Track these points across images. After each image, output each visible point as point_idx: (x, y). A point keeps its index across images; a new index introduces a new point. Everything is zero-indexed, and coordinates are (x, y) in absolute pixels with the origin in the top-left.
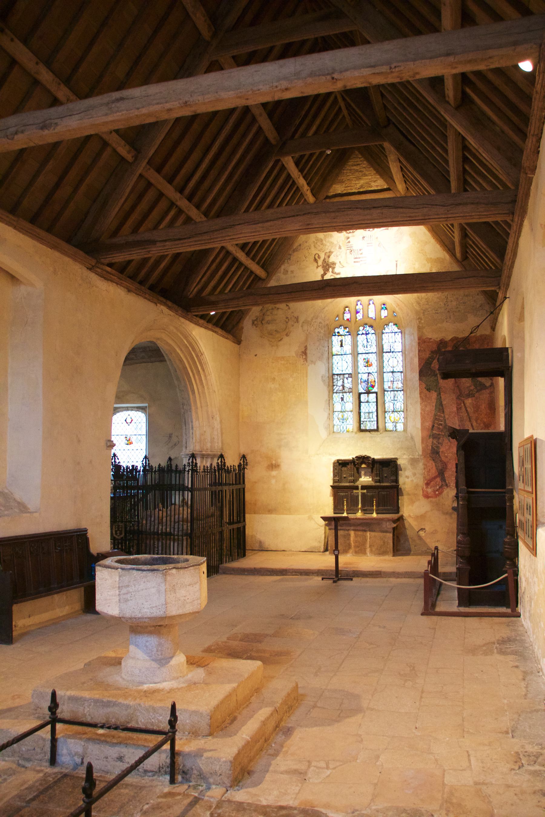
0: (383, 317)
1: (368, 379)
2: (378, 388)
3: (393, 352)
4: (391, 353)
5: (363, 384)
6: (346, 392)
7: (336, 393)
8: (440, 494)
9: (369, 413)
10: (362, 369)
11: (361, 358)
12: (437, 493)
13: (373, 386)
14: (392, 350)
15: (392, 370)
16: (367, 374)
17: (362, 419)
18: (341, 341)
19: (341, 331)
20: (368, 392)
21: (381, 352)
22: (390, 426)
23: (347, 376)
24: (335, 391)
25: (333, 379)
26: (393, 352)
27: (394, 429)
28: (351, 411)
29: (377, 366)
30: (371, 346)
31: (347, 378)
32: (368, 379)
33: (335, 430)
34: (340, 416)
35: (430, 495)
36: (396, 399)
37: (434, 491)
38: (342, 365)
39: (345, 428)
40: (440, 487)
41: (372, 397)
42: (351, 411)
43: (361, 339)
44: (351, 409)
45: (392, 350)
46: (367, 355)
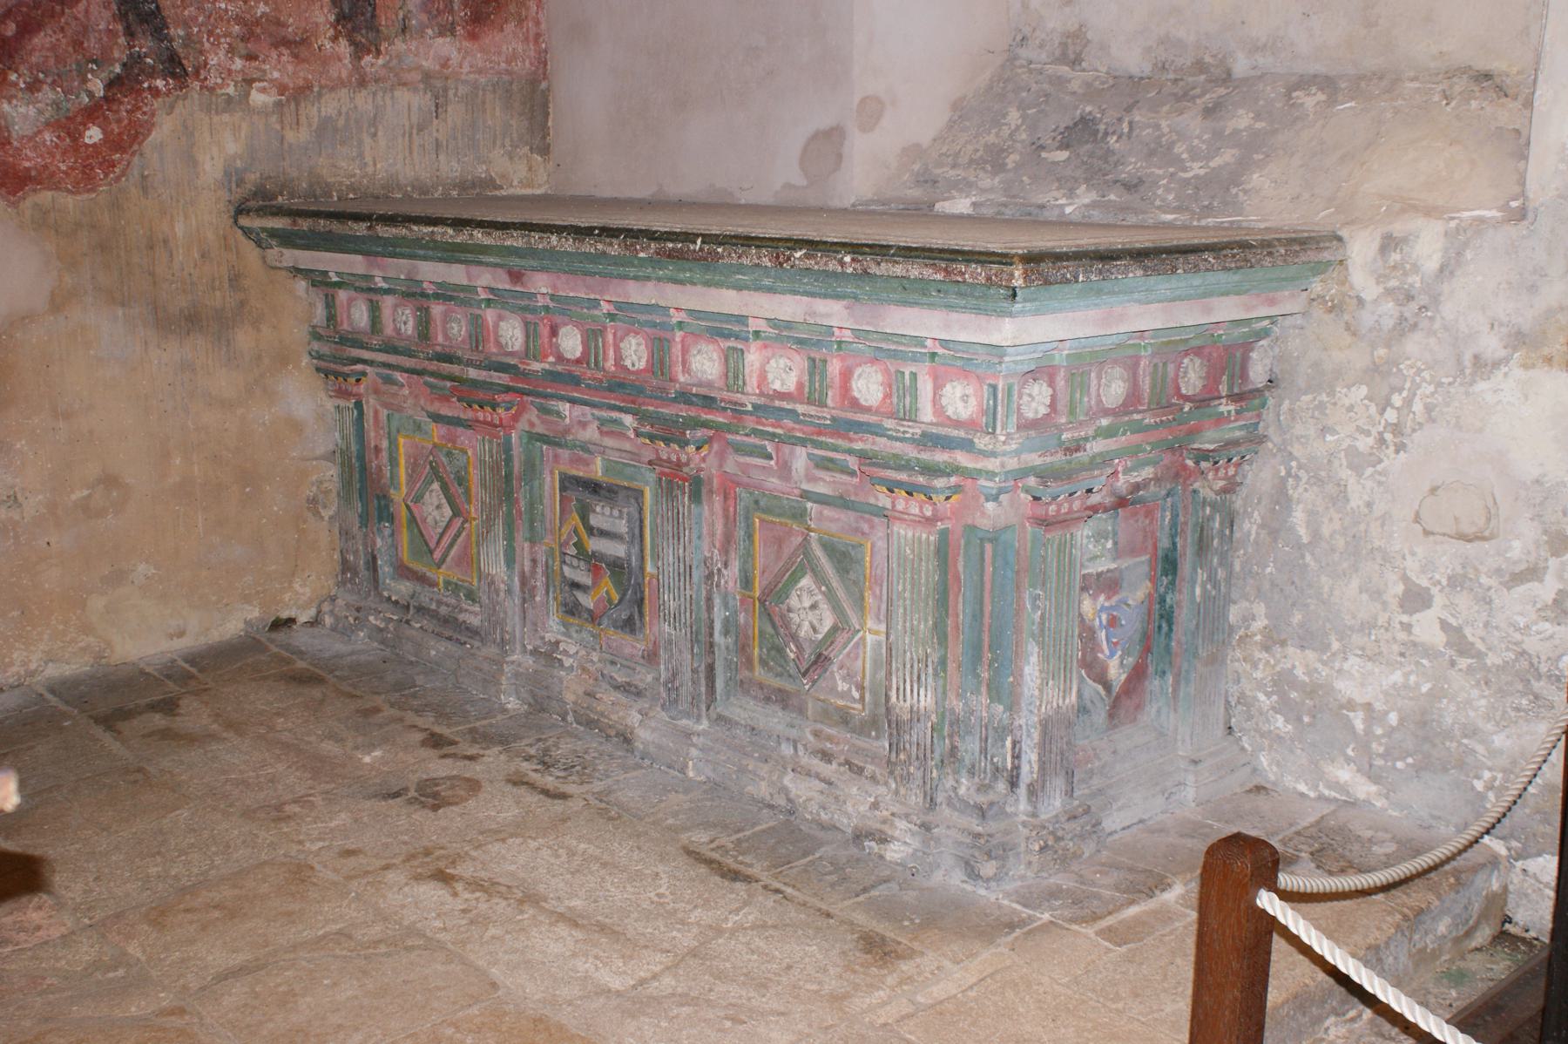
8: (126, 141)
12: (94, 135)
35: (30, 161)
37: (69, 127)
40: (109, 86)
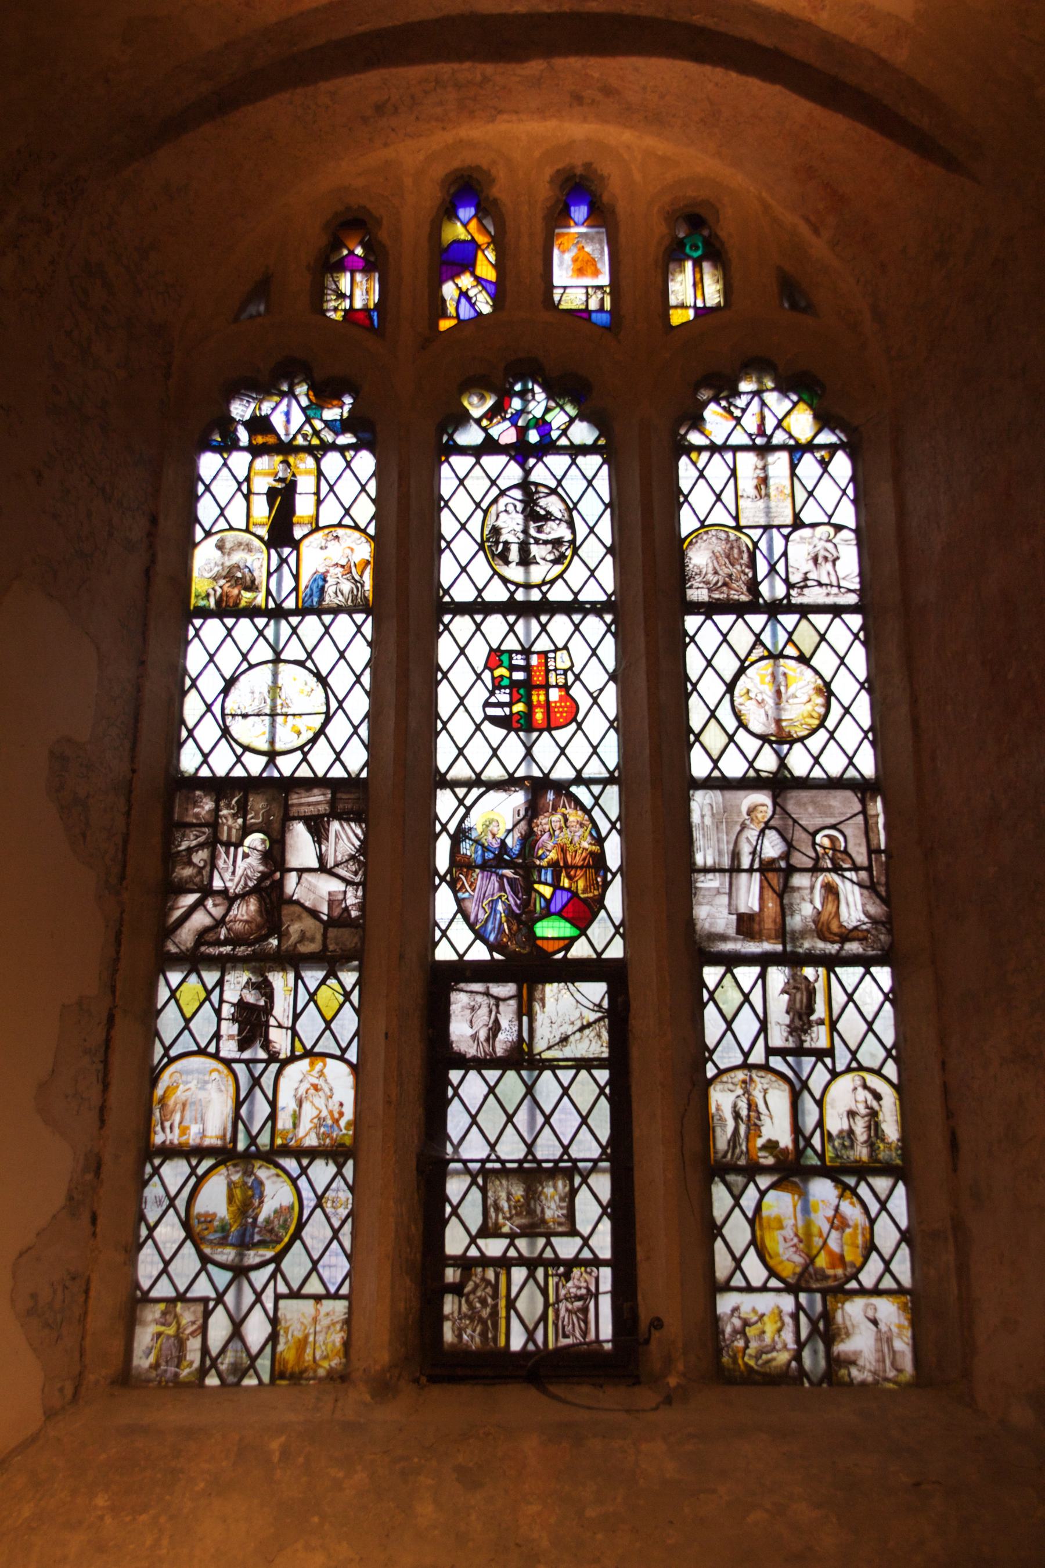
0: (677, 318)
1: (529, 840)
2: (624, 929)
3: (774, 609)
4: (757, 621)
5: (484, 886)
6: (293, 961)
7: (193, 961)
9: (531, 1173)
10: (466, 736)
11: (463, 653)
13: (583, 913)
14: (772, 590)
15: (768, 762)
16: (518, 798)
17: (455, 1242)
18: (283, 497)
19: (287, 416)
20: (527, 967)
21: (652, 605)
22: (759, 1314)
23: (317, 800)
24: (186, 935)
25: (175, 827)
26: (774, 609)
27: (812, 1360)
28: (335, 1153)
29: (620, 724)
30: (564, 552)
31: (318, 831)
32: (529, 840)
33: (142, 1361)
34: (215, 1198)
36: (819, 1037)
38: (267, 698)
39: (256, 1330)
41: (568, 1011)
42: (335, 1153)
43: (469, 488)
44: (344, 1131)
45: (772, 590)
46: (528, 628)
